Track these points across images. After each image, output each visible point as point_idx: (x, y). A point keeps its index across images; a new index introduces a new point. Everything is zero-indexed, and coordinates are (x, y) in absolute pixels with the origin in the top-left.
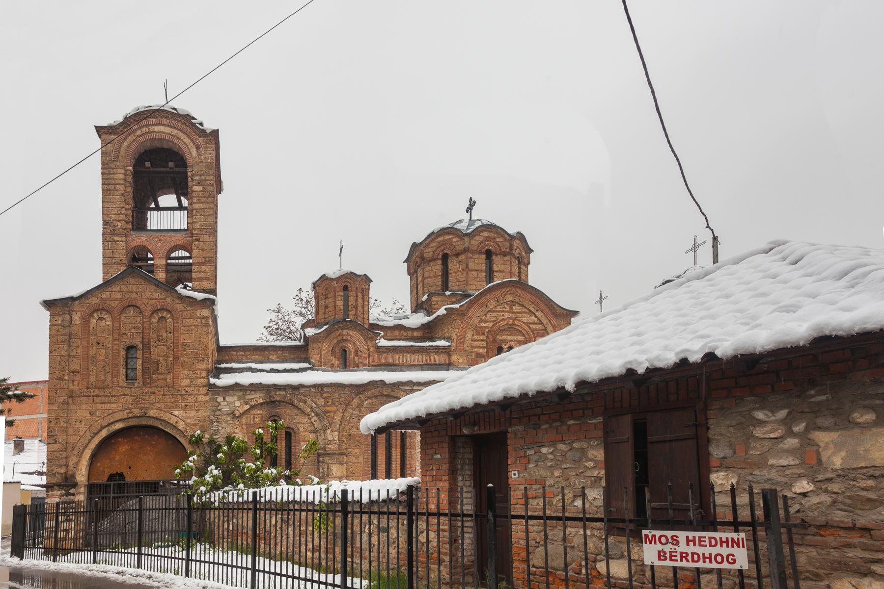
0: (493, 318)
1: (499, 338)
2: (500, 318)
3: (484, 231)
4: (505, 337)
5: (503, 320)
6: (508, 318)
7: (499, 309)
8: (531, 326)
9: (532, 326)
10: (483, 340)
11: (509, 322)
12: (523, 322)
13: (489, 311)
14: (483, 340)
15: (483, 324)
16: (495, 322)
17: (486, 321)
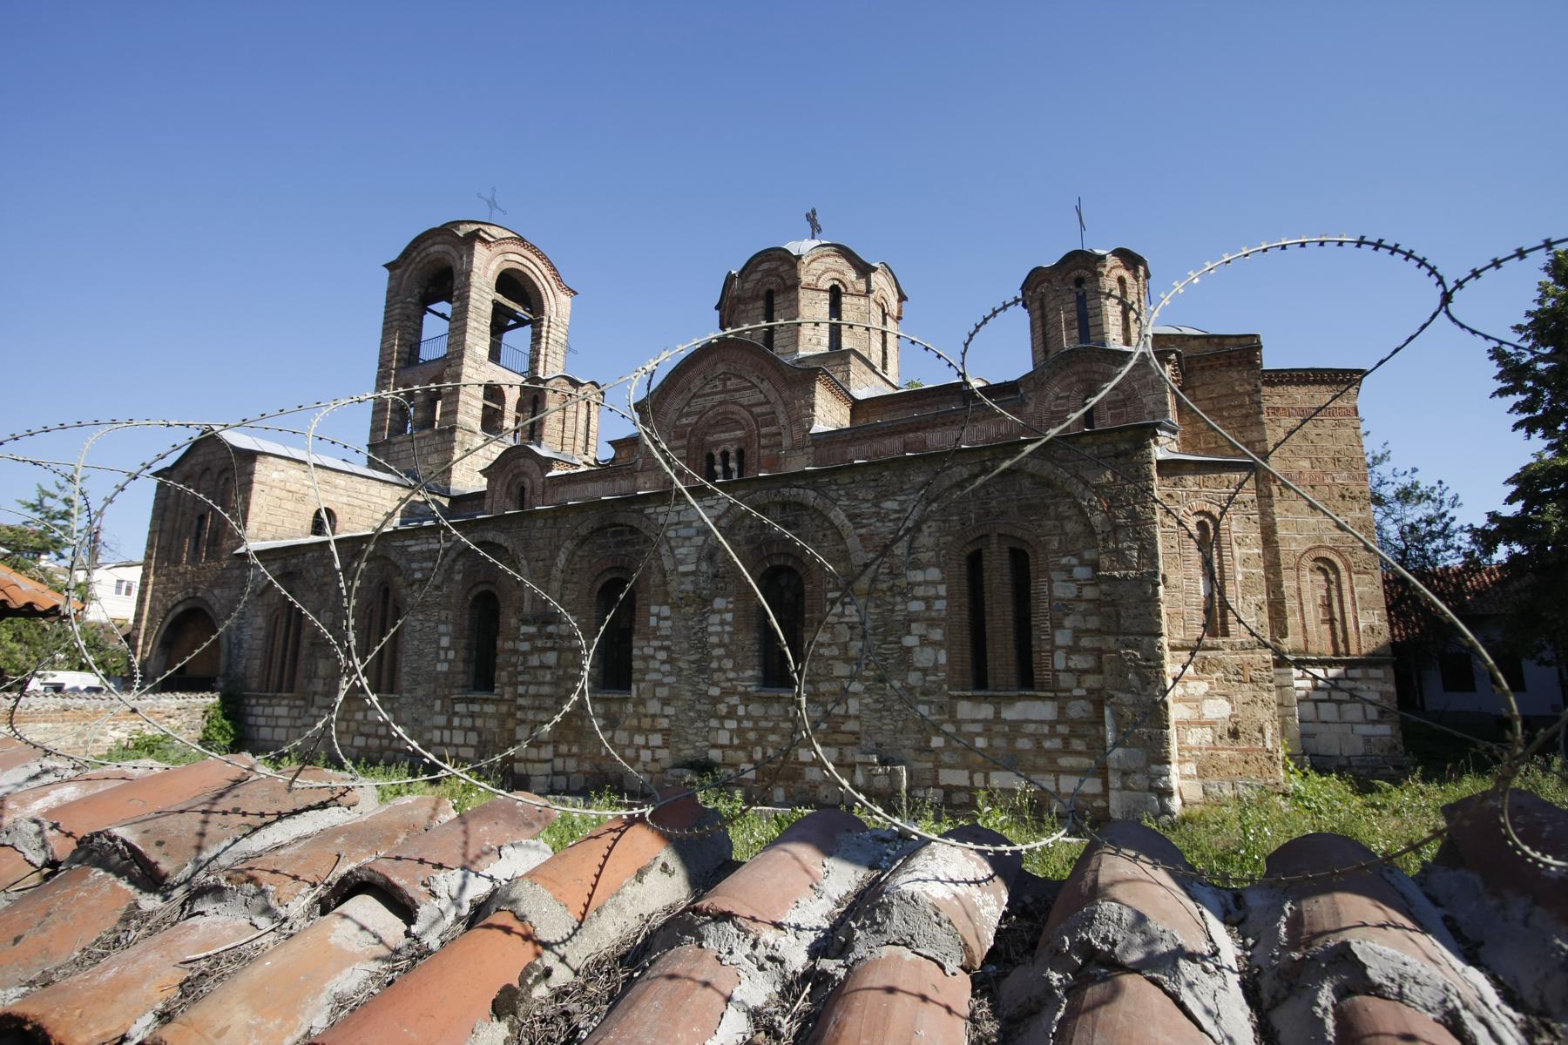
0: (698, 408)
1: (710, 438)
2: (709, 405)
3: (762, 262)
4: (717, 437)
5: (713, 407)
6: (721, 403)
7: (707, 390)
8: (754, 409)
9: (757, 410)
10: (683, 447)
11: (721, 409)
12: (742, 406)
13: (695, 396)
14: (683, 447)
15: (684, 421)
16: (702, 413)
17: (688, 415)
